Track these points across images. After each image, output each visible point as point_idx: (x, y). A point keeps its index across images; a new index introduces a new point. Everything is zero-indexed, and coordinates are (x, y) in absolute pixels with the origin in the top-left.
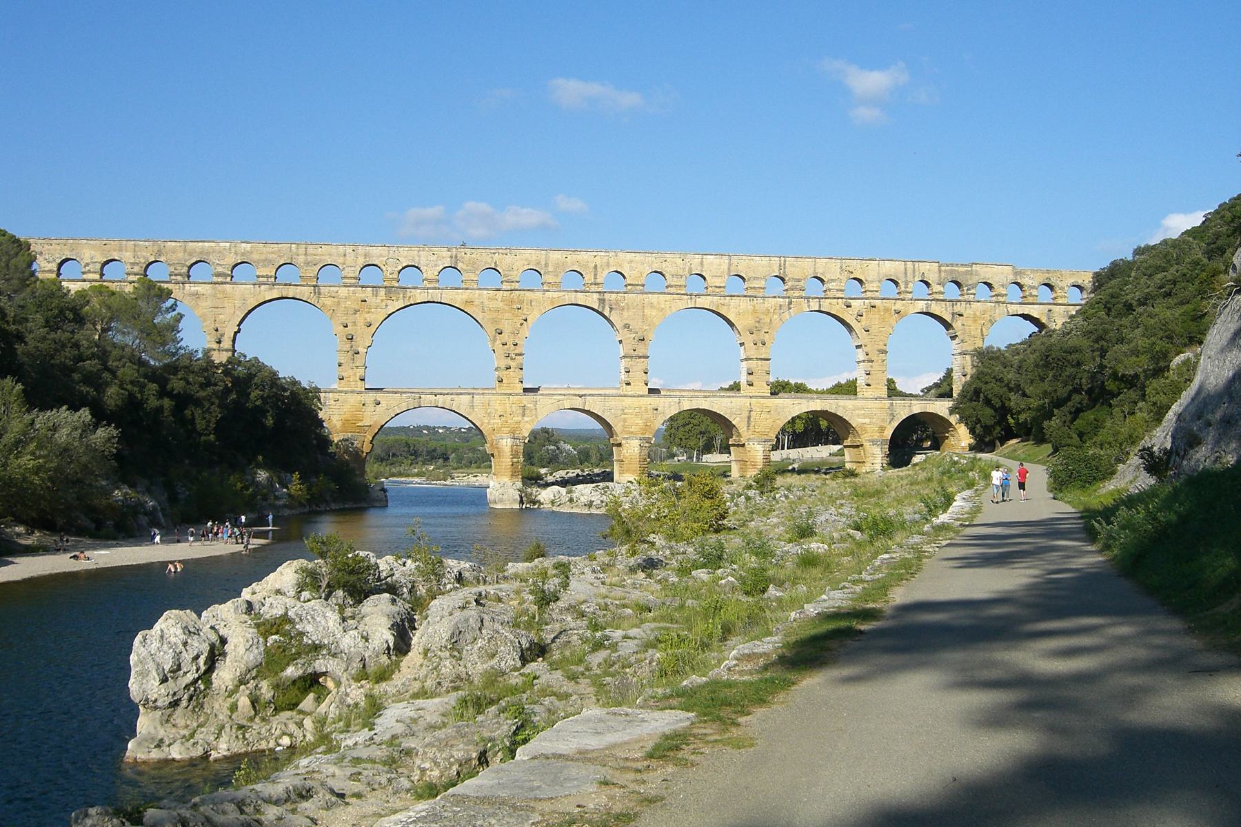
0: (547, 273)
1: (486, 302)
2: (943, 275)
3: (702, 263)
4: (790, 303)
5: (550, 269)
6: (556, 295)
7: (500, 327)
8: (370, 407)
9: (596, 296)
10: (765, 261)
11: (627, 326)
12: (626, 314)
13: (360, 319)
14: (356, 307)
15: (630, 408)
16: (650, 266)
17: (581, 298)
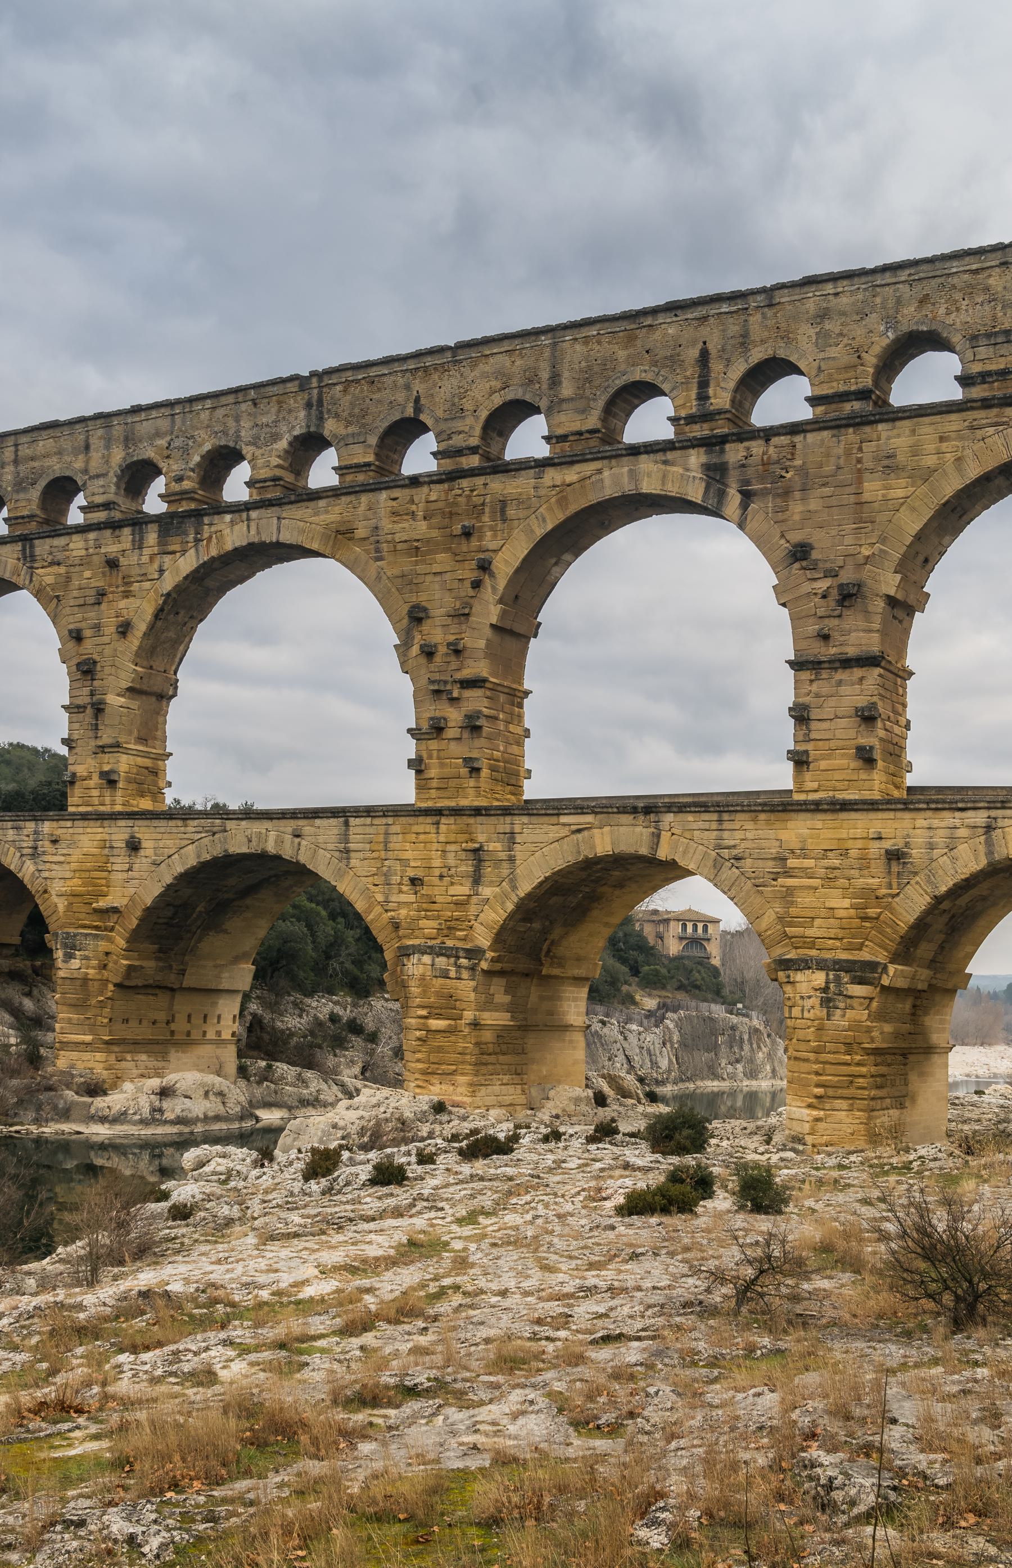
1: (386, 525)
5: (567, 390)
6: (571, 475)
7: (422, 598)
9: (696, 458)
12: (796, 509)
13: (108, 617)
14: (99, 583)
15: (804, 853)
16: (891, 321)
17: (649, 477)
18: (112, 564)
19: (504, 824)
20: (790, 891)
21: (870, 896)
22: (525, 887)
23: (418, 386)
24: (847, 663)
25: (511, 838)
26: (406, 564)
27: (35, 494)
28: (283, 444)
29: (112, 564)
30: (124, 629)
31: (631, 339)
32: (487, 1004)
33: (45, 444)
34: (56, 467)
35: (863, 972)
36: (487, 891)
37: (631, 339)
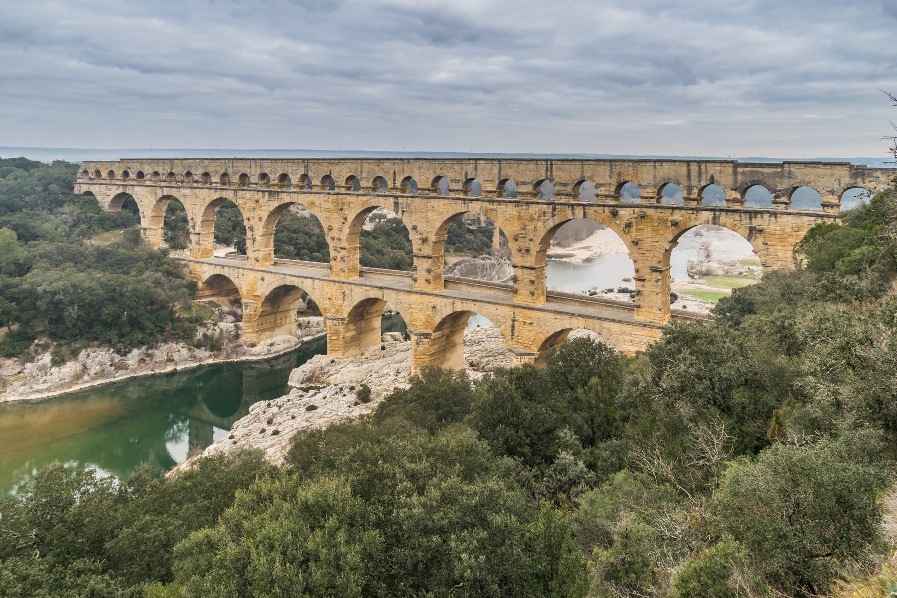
0: (362, 178)
2: (740, 178)
3: (476, 169)
4: (554, 210)
5: (364, 175)
6: (365, 199)
8: (260, 282)
9: (392, 200)
10: (532, 166)
11: (415, 228)
12: (414, 216)
14: (254, 205)
16: (434, 172)
18: (257, 201)
19: (350, 286)
20: (412, 313)
21: (429, 317)
22: (355, 303)
23: (331, 167)
24: (424, 257)
25: (351, 290)
26: (327, 214)
27: (238, 177)
28: (299, 176)
29: (257, 201)
30: (260, 219)
31: (378, 165)
32: (348, 330)
33: (240, 164)
34: (243, 170)
35: (426, 336)
36: (346, 303)
37: (378, 165)
